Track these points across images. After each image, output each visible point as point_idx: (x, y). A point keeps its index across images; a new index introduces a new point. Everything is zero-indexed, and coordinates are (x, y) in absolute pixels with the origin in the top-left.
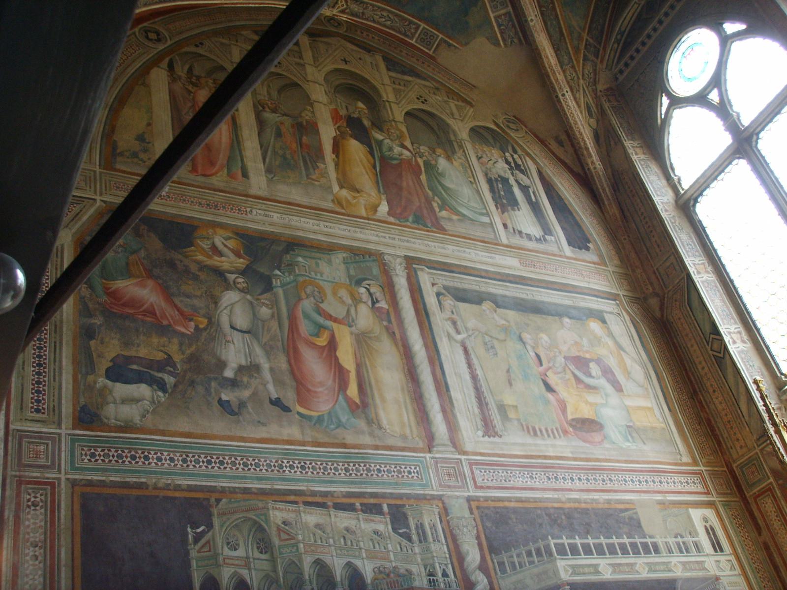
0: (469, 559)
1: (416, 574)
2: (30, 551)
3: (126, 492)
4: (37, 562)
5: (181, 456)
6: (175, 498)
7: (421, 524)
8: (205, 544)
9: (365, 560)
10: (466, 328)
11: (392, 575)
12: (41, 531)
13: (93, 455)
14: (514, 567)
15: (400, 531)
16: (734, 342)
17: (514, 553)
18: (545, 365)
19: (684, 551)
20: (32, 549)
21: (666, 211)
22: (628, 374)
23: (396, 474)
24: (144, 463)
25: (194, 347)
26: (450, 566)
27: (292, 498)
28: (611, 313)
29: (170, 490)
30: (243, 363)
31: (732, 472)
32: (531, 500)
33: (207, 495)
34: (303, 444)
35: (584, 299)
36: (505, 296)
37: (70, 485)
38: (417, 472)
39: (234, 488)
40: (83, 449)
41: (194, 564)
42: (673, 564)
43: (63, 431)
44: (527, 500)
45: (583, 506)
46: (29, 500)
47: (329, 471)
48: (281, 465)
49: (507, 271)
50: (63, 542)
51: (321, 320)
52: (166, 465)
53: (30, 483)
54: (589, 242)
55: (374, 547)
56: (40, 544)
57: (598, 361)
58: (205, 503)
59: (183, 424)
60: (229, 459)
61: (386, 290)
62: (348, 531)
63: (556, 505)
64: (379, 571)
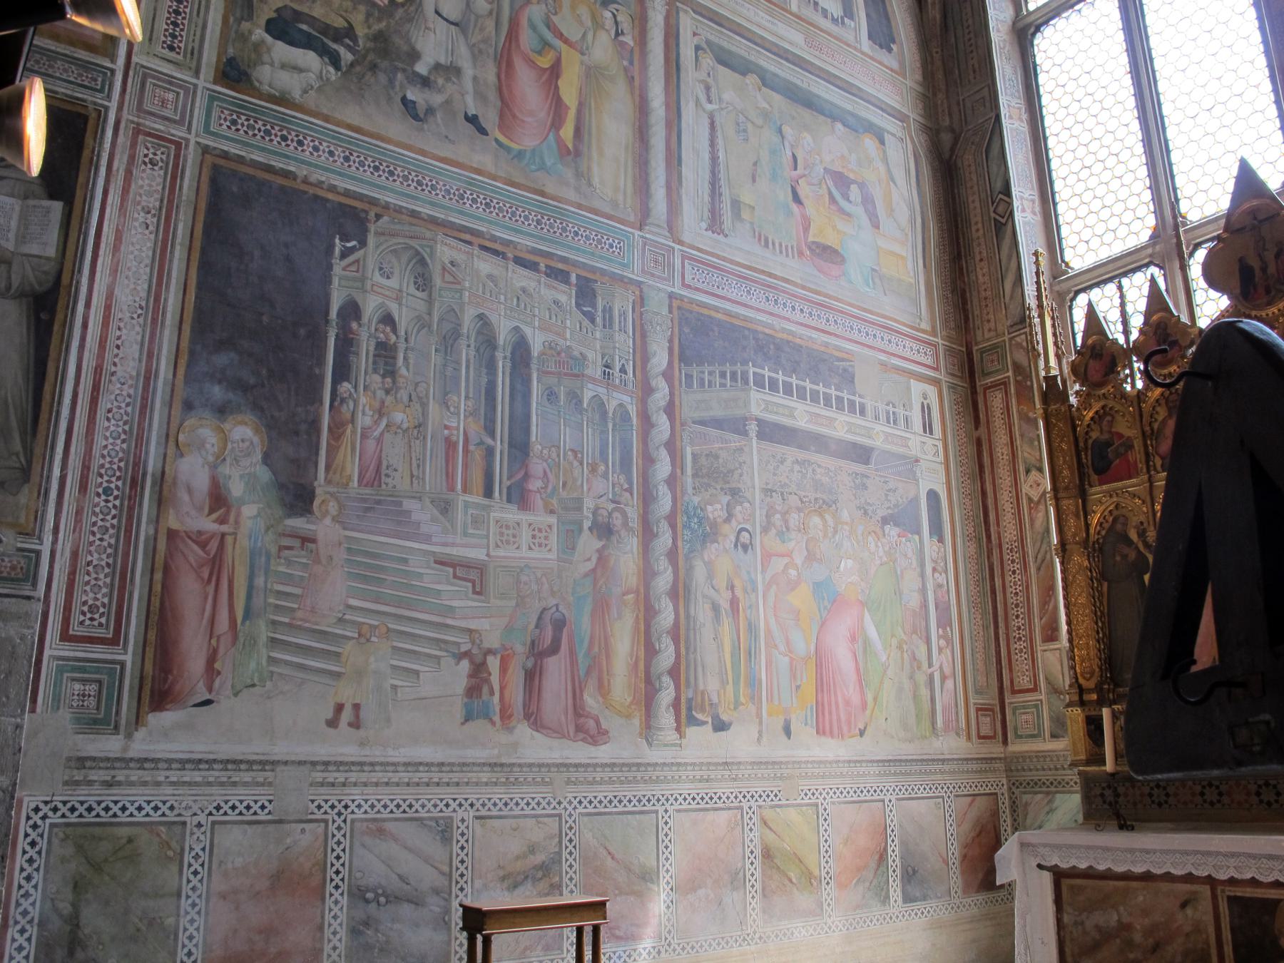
0: (654, 361)
3: (267, 176)
4: (147, 232)
5: (344, 152)
6: (327, 200)
8: (354, 262)
10: (720, 99)
11: (563, 354)
12: (158, 196)
13: (234, 122)
14: (702, 384)
15: (585, 309)
16: (1023, 210)
17: (707, 369)
18: (800, 171)
20: (142, 214)
21: (998, 31)
22: (891, 211)
24: (296, 148)
25: (384, 24)
27: (467, 237)
28: (893, 135)
29: (322, 188)
30: (442, 61)
31: (970, 354)
33: (366, 207)
34: (494, 178)
35: (868, 108)
36: (776, 75)
37: (200, 151)
40: (222, 112)
41: (336, 281)
43: (201, 83)
44: (737, 316)
45: (798, 341)
46: (146, 156)
49: (787, 46)
50: (181, 216)
51: (549, 36)
52: (323, 158)
53: (150, 135)
54: (894, 42)
55: (550, 318)
56: (153, 212)
57: (862, 186)
58: (363, 215)
59: (352, 114)
61: (637, 22)
63: (767, 331)
64: (550, 346)
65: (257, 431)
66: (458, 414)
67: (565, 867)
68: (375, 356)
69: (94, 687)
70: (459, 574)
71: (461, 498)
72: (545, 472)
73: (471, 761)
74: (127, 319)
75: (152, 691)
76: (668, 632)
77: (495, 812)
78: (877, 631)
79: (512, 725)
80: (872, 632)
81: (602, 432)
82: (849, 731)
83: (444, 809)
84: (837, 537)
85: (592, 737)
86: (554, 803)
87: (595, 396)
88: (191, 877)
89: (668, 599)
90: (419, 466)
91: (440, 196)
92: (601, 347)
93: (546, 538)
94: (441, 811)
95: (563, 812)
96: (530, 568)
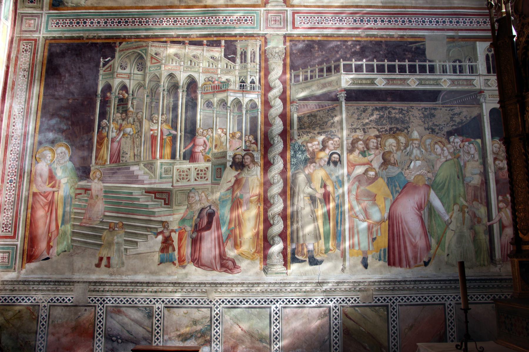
2: (22, 73)
6: (97, 43)
8: (109, 67)
11: (216, 82)
12: (28, 63)
13: (58, 23)
15: (229, 56)
19: (458, 71)
27: (164, 39)
32: (335, 36)
39: (131, 36)
41: (101, 77)
42: (443, 80)
46: (23, 49)
50: (37, 69)
53: (25, 40)
58: (113, 45)
65: (67, 148)
66: (158, 123)
67: (213, 332)
68: (118, 105)
69: (7, 254)
72: (205, 142)
73: (163, 281)
74: (17, 114)
75: (27, 255)
76: (279, 214)
77: (175, 305)
78: (442, 202)
79: (184, 265)
80: (437, 203)
81: (239, 116)
82: (416, 262)
83: (149, 303)
84: (408, 149)
85: (230, 270)
86: (208, 302)
88: (41, 326)
89: (279, 197)
91: (151, 25)
92: (239, 73)
93: (205, 174)
94: (148, 304)
95: (213, 306)
96: (195, 189)
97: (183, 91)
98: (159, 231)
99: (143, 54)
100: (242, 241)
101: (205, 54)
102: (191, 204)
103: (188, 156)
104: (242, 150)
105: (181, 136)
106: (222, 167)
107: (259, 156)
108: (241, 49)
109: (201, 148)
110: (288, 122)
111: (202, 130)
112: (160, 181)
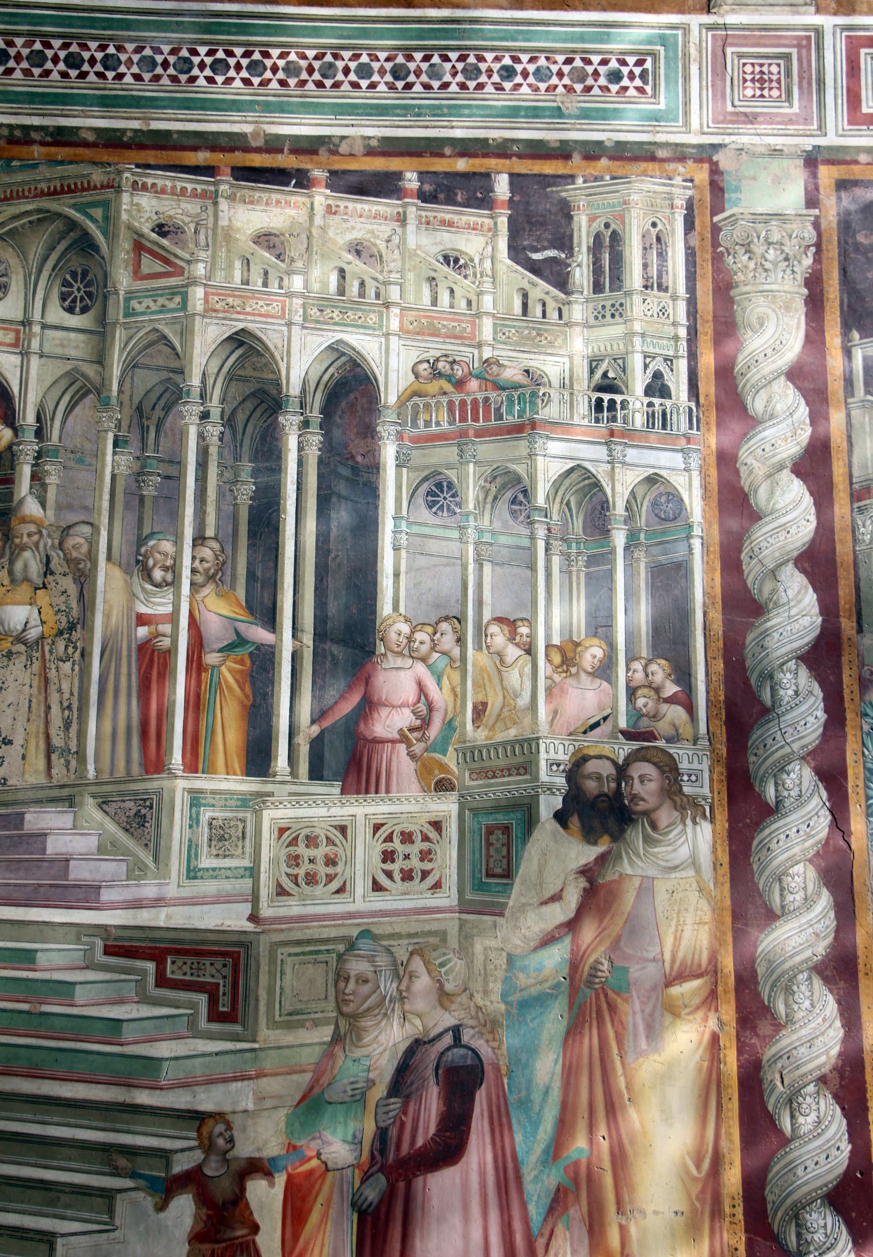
1: (555, 383)
7: (614, 232)
9: (394, 340)
11: (474, 384)
15: (536, 256)
23: (566, 81)
26: (682, 365)
27: (202, 157)
38: (643, 76)
39: (26, 128)
47: (340, 77)
48: (187, 61)
60: (26, 45)
62: (358, 253)
66: (175, 583)
70: (171, 971)
71: (181, 784)
72: (421, 688)
76: (822, 1080)
81: (592, 560)
87: (572, 470)
89: (817, 982)
90: (67, 724)
91: (128, 79)
93: (425, 855)
96: (375, 938)
97: (306, 424)
98: (177, 1169)
99: (92, 227)
100: (633, 1230)
101: (412, 240)
102: (354, 1017)
103: (334, 758)
104: (613, 736)
105: (296, 657)
106: (513, 820)
107: (705, 766)
108: (592, 219)
109: (403, 719)
110: (845, 591)
111: (405, 628)
112: (185, 892)
